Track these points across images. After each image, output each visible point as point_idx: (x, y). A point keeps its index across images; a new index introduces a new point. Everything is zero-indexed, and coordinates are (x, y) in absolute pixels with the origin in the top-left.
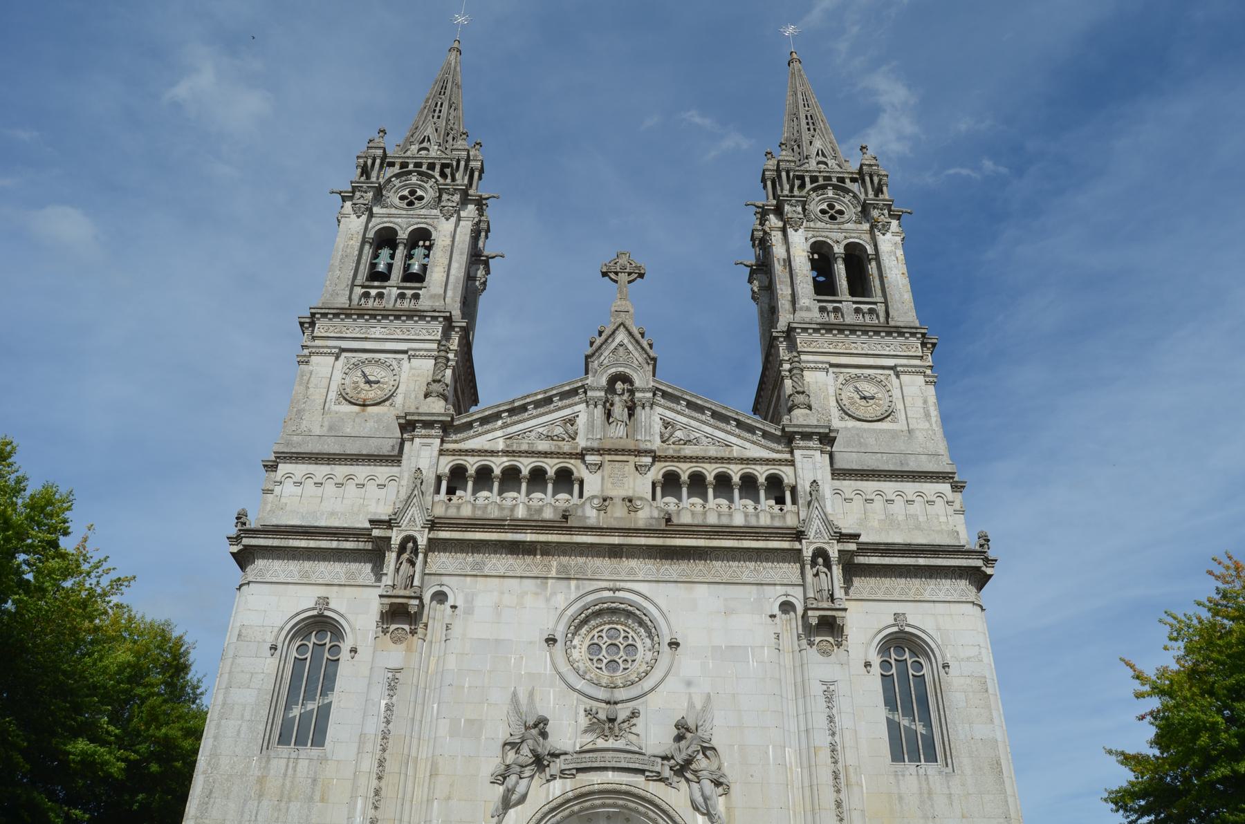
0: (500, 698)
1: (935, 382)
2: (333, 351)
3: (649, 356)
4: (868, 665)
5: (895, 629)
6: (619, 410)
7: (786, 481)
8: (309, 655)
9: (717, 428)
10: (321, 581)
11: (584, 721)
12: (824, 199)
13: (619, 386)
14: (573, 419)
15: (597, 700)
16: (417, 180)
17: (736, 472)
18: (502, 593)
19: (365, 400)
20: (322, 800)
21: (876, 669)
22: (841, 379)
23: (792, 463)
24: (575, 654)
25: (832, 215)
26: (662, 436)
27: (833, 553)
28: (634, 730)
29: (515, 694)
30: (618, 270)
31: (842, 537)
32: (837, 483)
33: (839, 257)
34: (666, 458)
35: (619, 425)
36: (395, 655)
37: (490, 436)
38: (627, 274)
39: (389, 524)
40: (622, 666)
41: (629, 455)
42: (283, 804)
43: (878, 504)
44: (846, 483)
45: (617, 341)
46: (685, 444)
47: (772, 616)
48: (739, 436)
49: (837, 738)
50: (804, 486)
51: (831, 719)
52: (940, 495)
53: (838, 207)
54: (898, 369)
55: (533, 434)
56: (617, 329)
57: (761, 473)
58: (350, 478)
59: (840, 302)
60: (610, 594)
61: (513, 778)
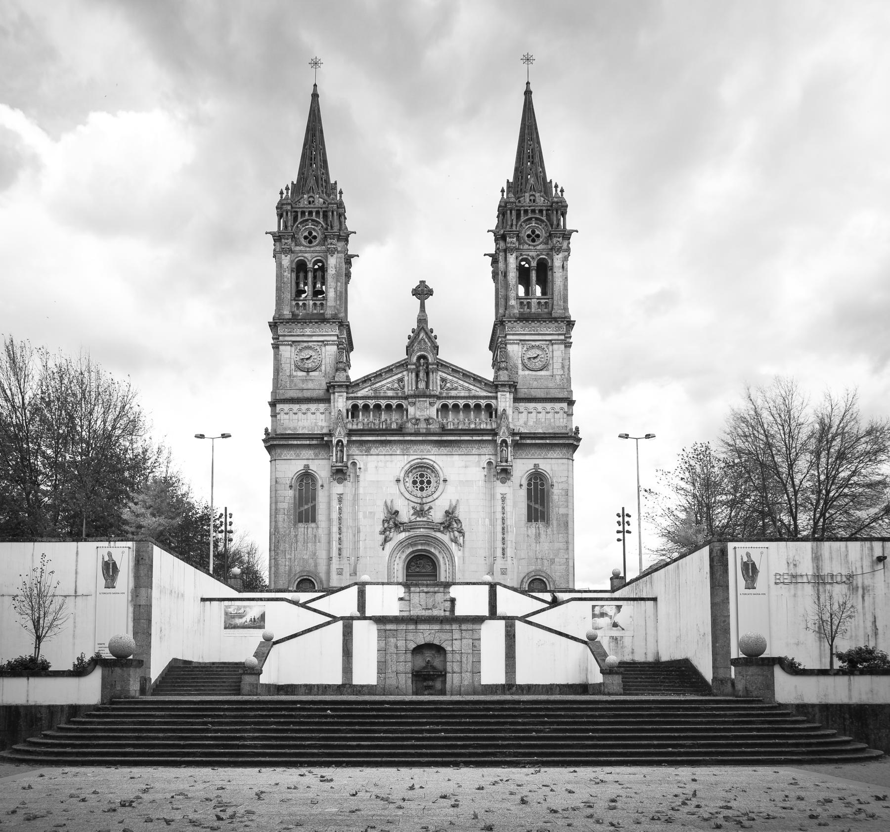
0: (381, 504)
4: (521, 485)
5: (534, 470)
8: (304, 487)
9: (465, 381)
10: (304, 458)
11: (412, 512)
12: (530, 227)
13: (422, 361)
15: (417, 503)
17: (472, 403)
18: (378, 462)
20: (319, 542)
21: (525, 487)
22: (525, 349)
23: (496, 398)
24: (407, 485)
25: (535, 236)
26: (441, 386)
27: (509, 441)
28: (430, 514)
29: (386, 502)
31: (514, 434)
36: (338, 488)
37: (366, 390)
40: (425, 489)
42: (305, 545)
43: (534, 414)
44: (521, 404)
45: (421, 337)
47: (484, 468)
48: (474, 386)
49: (505, 515)
50: (500, 410)
51: (503, 508)
52: (562, 409)
53: (537, 232)
55: (385, 387)
57: (483, 403)
58: (308, 409)
59: (531, 299)
60: (419, 461)
61: (388, 533)
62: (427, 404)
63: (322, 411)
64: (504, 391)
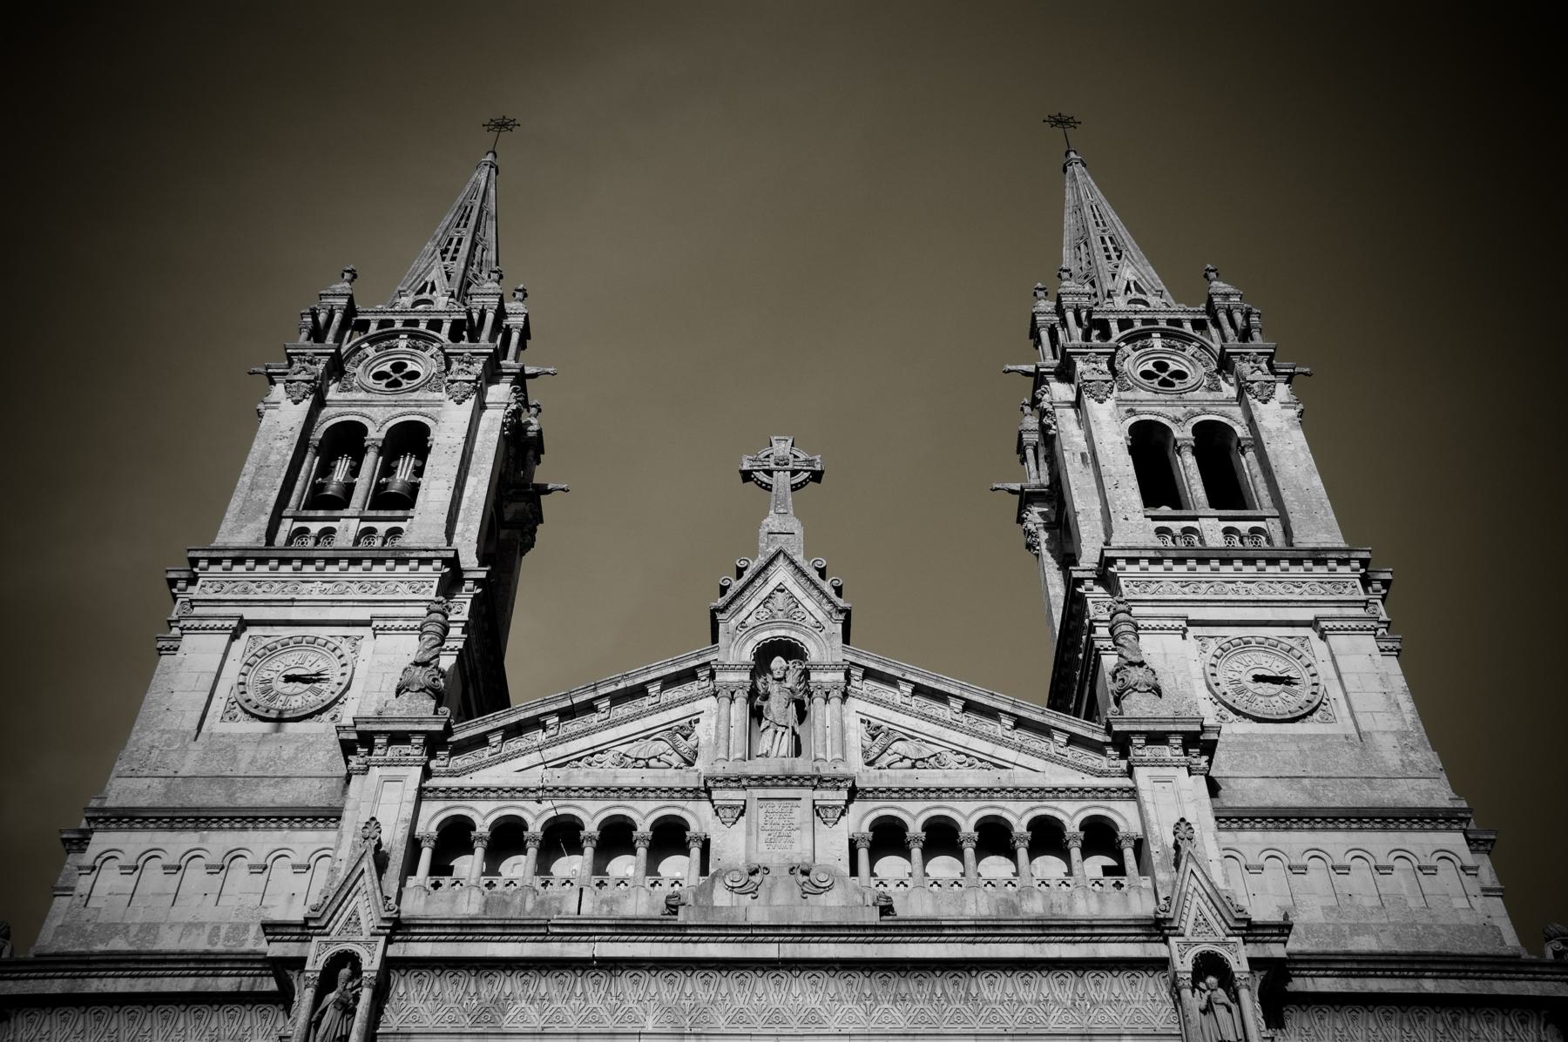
1: (1398, 651)
2: (227, 624)
3: (835, 606)
6: (778, 707)
7: (1123, 829)
9: (975, 734)
14: (688, 725)
16: (407, 347)
19: (281, 712)
22: (1212, 646)
23: (1132, 794)
26: (865, 753)
30: (773, 466)
31: (1250, 930)
32: (1227, 837)
33: (1186, 445)
34: (875, 793)
35: (779, 734)
37: (522, 762)
38: (788, 473)
39: (304, 930)
41: (801, 785)
46: (913, 766)
48: (1020, 749)
50: (1162, 838)
52: (1445, 855)
53: (1173, 367)
54: (1323, 624)
55: (608, 756)
56: (771, 562)
57: (1071, 815)
59: (1195, 518)
62: (803, 812)
63: (297, 859)
64: (1161, 763)
